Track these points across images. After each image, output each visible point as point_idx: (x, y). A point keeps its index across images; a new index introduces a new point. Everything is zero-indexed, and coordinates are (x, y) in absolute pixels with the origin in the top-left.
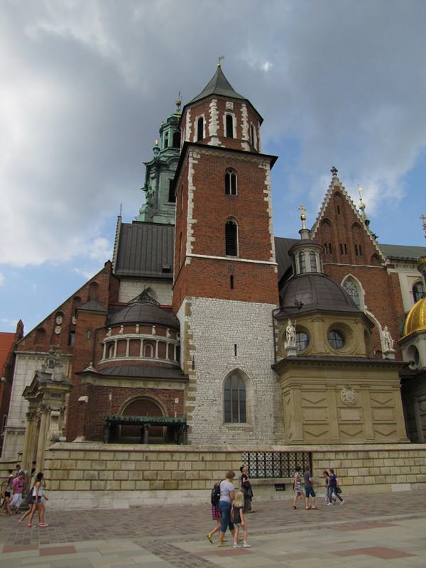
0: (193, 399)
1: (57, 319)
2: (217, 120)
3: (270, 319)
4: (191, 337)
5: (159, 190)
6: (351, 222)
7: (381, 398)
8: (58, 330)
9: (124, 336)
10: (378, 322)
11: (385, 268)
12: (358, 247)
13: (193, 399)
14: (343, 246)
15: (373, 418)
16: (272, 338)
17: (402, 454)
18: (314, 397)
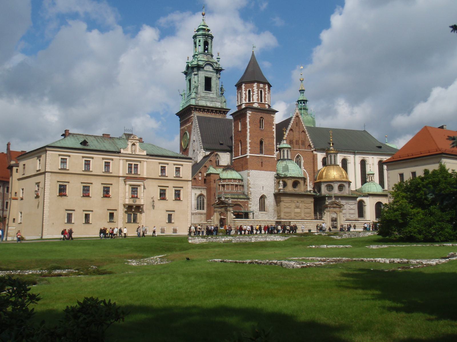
0: (251, 204)
1: (199, 174)
2: (257, 94)
3: (274, 177)
4: (250, 184)
5: (199, 82)
6: (301, 130)
7: (307, 205)
8: (200, 178)
9: (228, 183)
10: (307, 174)
11: (312, 151)
12: (303, 141)
13: (251, 204)
14: (297, 141)
15: (304, 211)
16: (274, 184)
17: (313, 223)
18: (287, 205)
